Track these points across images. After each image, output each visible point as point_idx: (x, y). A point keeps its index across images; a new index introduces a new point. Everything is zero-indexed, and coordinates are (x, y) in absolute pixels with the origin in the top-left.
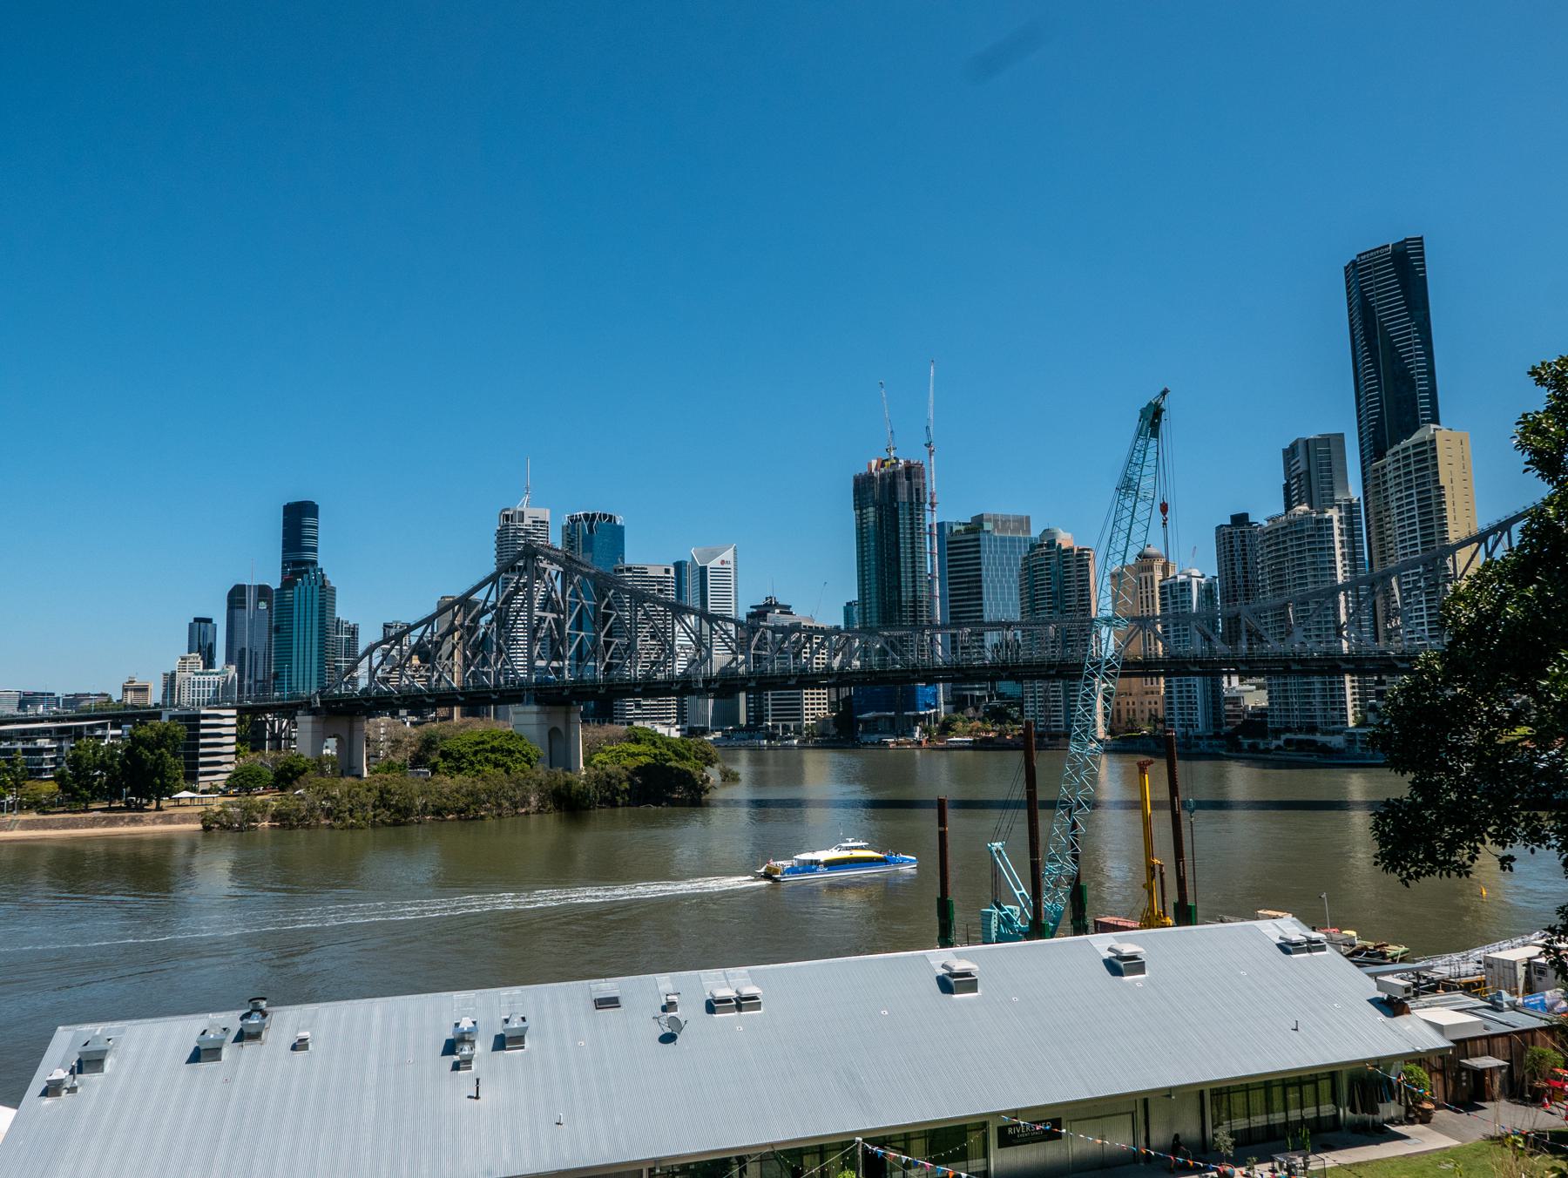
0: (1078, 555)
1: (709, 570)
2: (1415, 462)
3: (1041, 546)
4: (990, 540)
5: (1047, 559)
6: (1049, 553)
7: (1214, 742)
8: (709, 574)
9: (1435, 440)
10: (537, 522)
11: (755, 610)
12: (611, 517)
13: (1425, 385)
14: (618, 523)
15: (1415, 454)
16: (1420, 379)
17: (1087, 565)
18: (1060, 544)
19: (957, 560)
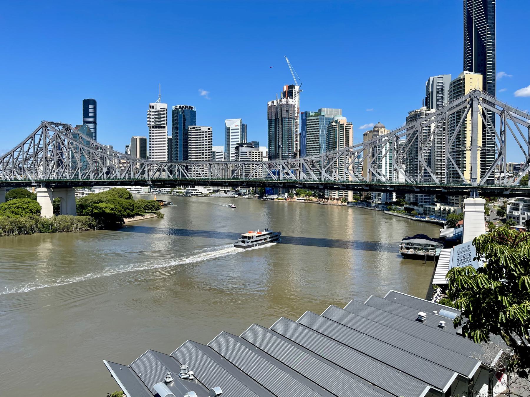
0: (346, 126)
1: (230, 129)
2: (457, 88)
3: (332, 122)
4: (324, 119)
5: (334, 128)
6: (334, 126)
7: (384, 206)
8: (230, 130)
9: (464, 79)
10: (162, 109)
11: (238, 145)
12: (190, 107)
13: (491, 53)
14: (194, 110)
15: (457, 85)
16: (488, 50)
17: (349, 131)
18: (339, 122)
19: (310, 127)
